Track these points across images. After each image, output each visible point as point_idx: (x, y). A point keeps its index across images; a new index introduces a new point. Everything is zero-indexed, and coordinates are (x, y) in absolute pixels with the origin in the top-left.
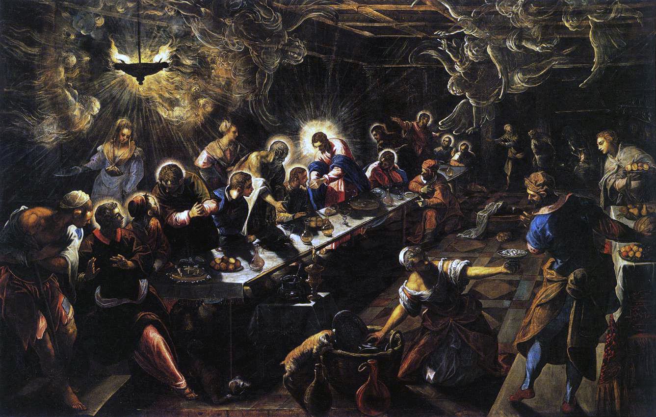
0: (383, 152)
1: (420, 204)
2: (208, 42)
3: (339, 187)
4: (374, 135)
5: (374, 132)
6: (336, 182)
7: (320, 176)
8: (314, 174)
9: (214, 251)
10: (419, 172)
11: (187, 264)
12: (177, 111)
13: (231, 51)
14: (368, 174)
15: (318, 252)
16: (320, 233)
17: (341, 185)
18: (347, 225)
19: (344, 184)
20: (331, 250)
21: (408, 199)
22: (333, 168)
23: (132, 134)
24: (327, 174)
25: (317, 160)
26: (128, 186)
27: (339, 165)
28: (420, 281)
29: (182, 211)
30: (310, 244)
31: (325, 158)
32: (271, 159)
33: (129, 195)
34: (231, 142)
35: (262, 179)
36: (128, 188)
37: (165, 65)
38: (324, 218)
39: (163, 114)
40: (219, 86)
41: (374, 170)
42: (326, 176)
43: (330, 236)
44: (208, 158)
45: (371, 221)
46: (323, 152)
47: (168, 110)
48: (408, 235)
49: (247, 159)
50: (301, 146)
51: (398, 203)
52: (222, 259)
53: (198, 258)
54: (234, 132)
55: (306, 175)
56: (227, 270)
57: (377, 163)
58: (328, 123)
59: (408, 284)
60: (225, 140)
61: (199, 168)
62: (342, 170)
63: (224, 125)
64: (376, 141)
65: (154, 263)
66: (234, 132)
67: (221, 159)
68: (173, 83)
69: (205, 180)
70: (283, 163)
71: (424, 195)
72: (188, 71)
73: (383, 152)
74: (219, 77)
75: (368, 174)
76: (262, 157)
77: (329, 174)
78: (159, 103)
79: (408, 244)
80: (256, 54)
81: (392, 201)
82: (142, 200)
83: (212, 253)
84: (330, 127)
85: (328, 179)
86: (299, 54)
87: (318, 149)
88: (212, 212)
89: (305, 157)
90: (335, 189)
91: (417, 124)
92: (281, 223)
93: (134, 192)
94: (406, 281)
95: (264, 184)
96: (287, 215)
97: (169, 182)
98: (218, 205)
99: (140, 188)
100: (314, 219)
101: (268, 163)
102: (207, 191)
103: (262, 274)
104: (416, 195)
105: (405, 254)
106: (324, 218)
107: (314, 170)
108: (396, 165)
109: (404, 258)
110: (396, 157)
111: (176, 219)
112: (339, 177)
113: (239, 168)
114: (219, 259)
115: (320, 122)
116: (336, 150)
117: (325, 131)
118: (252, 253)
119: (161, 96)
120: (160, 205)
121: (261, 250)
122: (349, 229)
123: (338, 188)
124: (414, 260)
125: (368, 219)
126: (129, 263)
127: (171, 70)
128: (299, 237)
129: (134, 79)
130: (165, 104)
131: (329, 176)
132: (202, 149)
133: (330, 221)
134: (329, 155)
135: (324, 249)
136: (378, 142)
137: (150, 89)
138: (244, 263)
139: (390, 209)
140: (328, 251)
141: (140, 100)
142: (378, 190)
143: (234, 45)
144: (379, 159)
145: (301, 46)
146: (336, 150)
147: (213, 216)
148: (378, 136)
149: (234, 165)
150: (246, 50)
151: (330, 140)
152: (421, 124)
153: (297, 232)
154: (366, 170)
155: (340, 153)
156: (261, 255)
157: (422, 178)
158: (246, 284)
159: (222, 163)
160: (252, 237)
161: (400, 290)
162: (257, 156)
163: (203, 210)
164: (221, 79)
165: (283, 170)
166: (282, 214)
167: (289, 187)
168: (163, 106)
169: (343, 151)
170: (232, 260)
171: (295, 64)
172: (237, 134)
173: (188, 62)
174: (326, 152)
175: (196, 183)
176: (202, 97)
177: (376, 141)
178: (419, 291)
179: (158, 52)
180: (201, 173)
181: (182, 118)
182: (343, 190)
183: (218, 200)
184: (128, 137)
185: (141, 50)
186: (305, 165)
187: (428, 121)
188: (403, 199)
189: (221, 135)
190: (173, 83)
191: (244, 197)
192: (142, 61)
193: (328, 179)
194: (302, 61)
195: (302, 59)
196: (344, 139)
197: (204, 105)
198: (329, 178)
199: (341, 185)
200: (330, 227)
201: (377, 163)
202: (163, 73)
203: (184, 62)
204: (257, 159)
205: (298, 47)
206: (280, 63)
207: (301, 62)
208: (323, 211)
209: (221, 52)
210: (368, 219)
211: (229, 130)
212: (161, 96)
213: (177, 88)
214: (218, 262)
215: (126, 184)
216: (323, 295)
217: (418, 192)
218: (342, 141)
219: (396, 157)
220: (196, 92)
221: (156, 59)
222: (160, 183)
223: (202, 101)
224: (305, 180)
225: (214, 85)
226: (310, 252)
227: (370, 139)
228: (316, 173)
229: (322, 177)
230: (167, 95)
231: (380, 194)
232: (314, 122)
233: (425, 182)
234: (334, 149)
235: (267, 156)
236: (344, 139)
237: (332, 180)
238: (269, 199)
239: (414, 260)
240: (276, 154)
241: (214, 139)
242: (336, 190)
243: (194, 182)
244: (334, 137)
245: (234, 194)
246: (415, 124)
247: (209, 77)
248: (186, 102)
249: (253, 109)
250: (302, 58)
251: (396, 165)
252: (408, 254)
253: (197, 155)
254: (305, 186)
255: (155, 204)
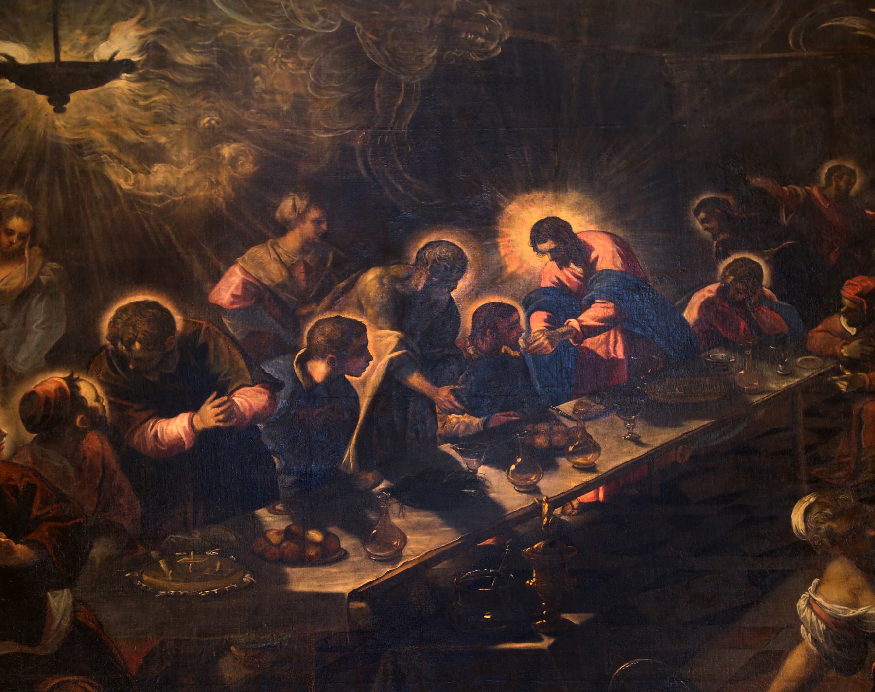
0: (730, 260)
1: (843, 386)
2: (244, 13)
3: (611, 348)
4: (703, 222)
5: (702, 215)
6: (602, 337)
7: (553, 322)
8: (539, 321)
9: (262, 512)
10: (836, 307)
11: (186, 548)
12: (160, 174)
13: (305, 33)
14: (691, 314)
15: (558, 511)
16: (563, 462)
17: (616, 342)
18: (637, 441)
19: (624, 341)
20: (596, 504)
21: (807, 375)
22: (591, 302)
23: (33, 232)
24: (576, 316)
25: (546, 283)
26: (22, 356)
27: (610, 297)
28: (857, 579)
29: (171, 413)
30: (534, 490)
31: (569, 279)
32: (420, 283)
33: (21, 378)
34: (306, 246)
35: (396, 333)
36: (22, 359)
37: (127, 66)
38: (571, 424)
39: (122, 182)
40: (275, 114)
41: (707, 305)
42: (573, 323)
43: (590, 468)
44: (245, 284)
45: (704, 430)
46: (562, 264)
47: (134, 171)
48: (816, 461)
49: (353, 284)
50: (503, 252)
51: (778, 385)
52: (288, 534)
53: (216, 531)
54: (317, 222)
55: (518, 321)
56: (302, 561)
57: (714, 287)
58: (573, 196)
59: (822, 589)
60: (291, 242)
61: (219, 309)
62: (618, 308)
63: (287, 206)
64: (707, 234)
65: (91, 547)
66: (317, 222)
67: (282, 286)
68: (147, 108)
69: (239, 338)
70: (453, 294)
71: (853, 364)
72: (191, 80)
73: (730, 260)
74: (273, 92)
75: (691, 314)
76: (395, 279)
77: (580, 318)
78: (111, 155)
79: (816, 485)
80: (374, 38)
81: (763, 379)
82: (60, 389)
83: (256, 519)
84: (578, 206)
85: (579, 329)
86: (489, 37)
87: (547, 258)
88: (257, 416)
89: (513, 277)
90: (601, 351)
91: (821, 190)
92: (452, 438)
93: (36, 371)
94: (816, 581)
95: (401, 344)
96: (465, 418)
97: (137, 345)
98: (273, 399)
99: (53, 360)
100: (543, 427)
101: (415, 294)
102: (242, 363)
103: (399, 567)
104: (830, 365)
105: (807, 511)
106: (571, 424)
107: (539, 308)
108: (768, 292)
109: (805, 521)
110: (765, 271)
111: (156, 435)
112: (607, 324)
113: (330, 308)
114: (279, 533)
115: (551, 195)
116: (597, 259)
117: (564, 214)
118: (372, 516)
119: (116, 139)
120: (110, 403)
121: (395, 507)
122: (643, 451)
123: (608, 350)
124: (834, 525)
125: (695, 425)
126: (21, 549)
127: (142, 78)
128: (504, 474)
129: (42, 99)
130: (125, 158)
131: (579, 322)
132: (230, 263)
133: (590, 431)
134: (578, 270)
135: (575, 503)
136: (714, 237)
137: (85, 124)
138: (347, 543)
139: (757, 399)
140: (584, 507)
141: (57, 149)
142: (721, 355)
143: (313, 18)
144: (719, 279)
145: (492, 18)
146: (597, 259)
147: (261, 426)
148: (714, 224)
149: (318, 299)
150: (347, 31)
151: (582, 237)
152: (831, 191)
153: (500, 463)
154: (683, 306)
155: (610, 267)
156: (396, 521)
157: (843, 322)
158: (355, 595)
159: (284, 295)
160: (370, 477)
161: (801, 604)
162: (380, 278)
163: (231, 411)
164: (278, 98)
165: (452, 312)
166: (453, 418)
167: (471, 351)
168: (120, 161)
169: (619, 261)
170: (315, 536)
171: (478, 59)
172: (324, 226)
173: (189, 59)
174: (572, 265)
175: (211, 346)
176: (229, 140)
177: (707, 234)
178: (856, 606)
179: (106, 37)
180: (227, 322)
181: (172, 191)
182: (620, 354)
183: (273, 386)
184: (22, 237)
185: (61, 33)
186: (514, 297)
187: (850, 184)
188: (791, 375)
189: (282, 229)
190: (147, 108)
191: (347, 376)
192: (64, 58)
193: (579, 329)
194: (500, 50)
195: (497, 47)
196: (620, 233)
197: (233, 160)
198: (582, 327)
199: (616, 342)
200: (590, 446)
201: (714, 287)
202: (122, 84)
203: (179, 60)
204: (382, 284)
205: (487, 20)
206: (438, 58)
207: (495, 55)
208: (567, 407)
209: (278, 35)
210: (695, 425)
211: (301, 217)
212: (116, 139)
213: (159, 120)
214: (274, 538)
215: (16, 351)
216: (574, 619)
217: (836, 357)
218: (614, 238)
219: (765, 271)
220: (211, 128)
221: (103, 52)
222: (111, 347)
223: (227, 151)
224: (515, 333)
225: (261, 111)
226: (537, 509)
227: (692, 232)
228: (543, 315)
229: (561, 325)
230: (131, 137)
231: (724, 365)
232: (537, 195)
233: (852, 331)
234: (593, 255)
235: (409, 277)
236: (620, 233)
237: (589, 331)
238: (416, 380)
239: (834, 525)
240: (433, 272)
241: (262, 239)
242: (603, 355)
243: (205, 346)
244: (592, 228)
245: (319, 370)
246: (815, 191)
247: (247, 92)
248: (185, 152)
249: (365, 163)
250: (499, 44)
251: (768, 292)
252: (815, 510)
253: (216, 276)
254: (515, 347)
255: (98, 399)
